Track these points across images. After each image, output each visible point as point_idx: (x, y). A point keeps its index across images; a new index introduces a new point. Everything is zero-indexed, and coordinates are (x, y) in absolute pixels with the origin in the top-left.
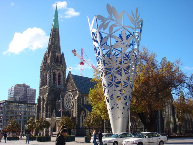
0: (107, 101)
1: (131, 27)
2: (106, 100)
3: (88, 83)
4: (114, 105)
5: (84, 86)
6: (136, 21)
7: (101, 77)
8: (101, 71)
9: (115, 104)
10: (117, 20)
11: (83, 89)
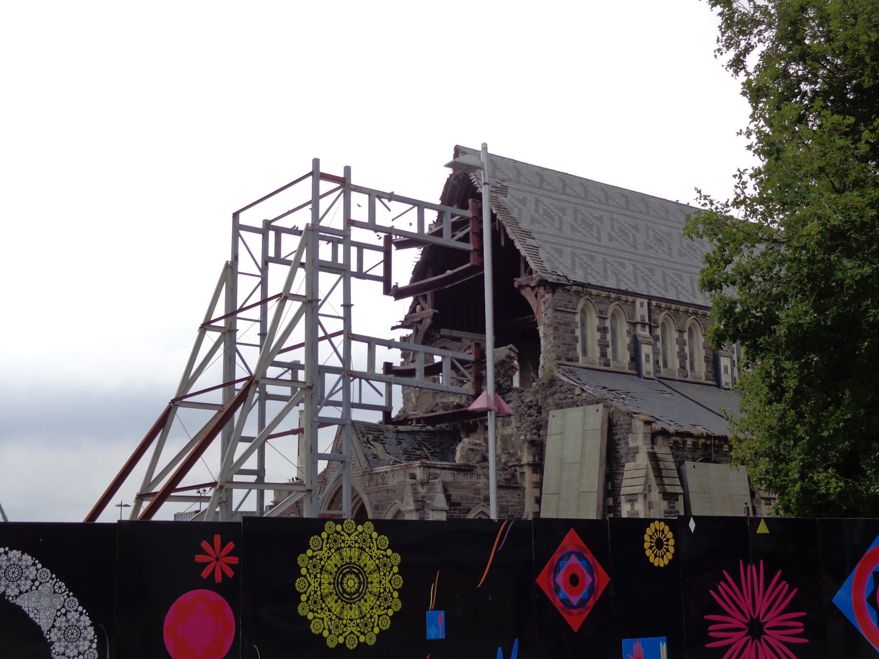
11: (560, 252)
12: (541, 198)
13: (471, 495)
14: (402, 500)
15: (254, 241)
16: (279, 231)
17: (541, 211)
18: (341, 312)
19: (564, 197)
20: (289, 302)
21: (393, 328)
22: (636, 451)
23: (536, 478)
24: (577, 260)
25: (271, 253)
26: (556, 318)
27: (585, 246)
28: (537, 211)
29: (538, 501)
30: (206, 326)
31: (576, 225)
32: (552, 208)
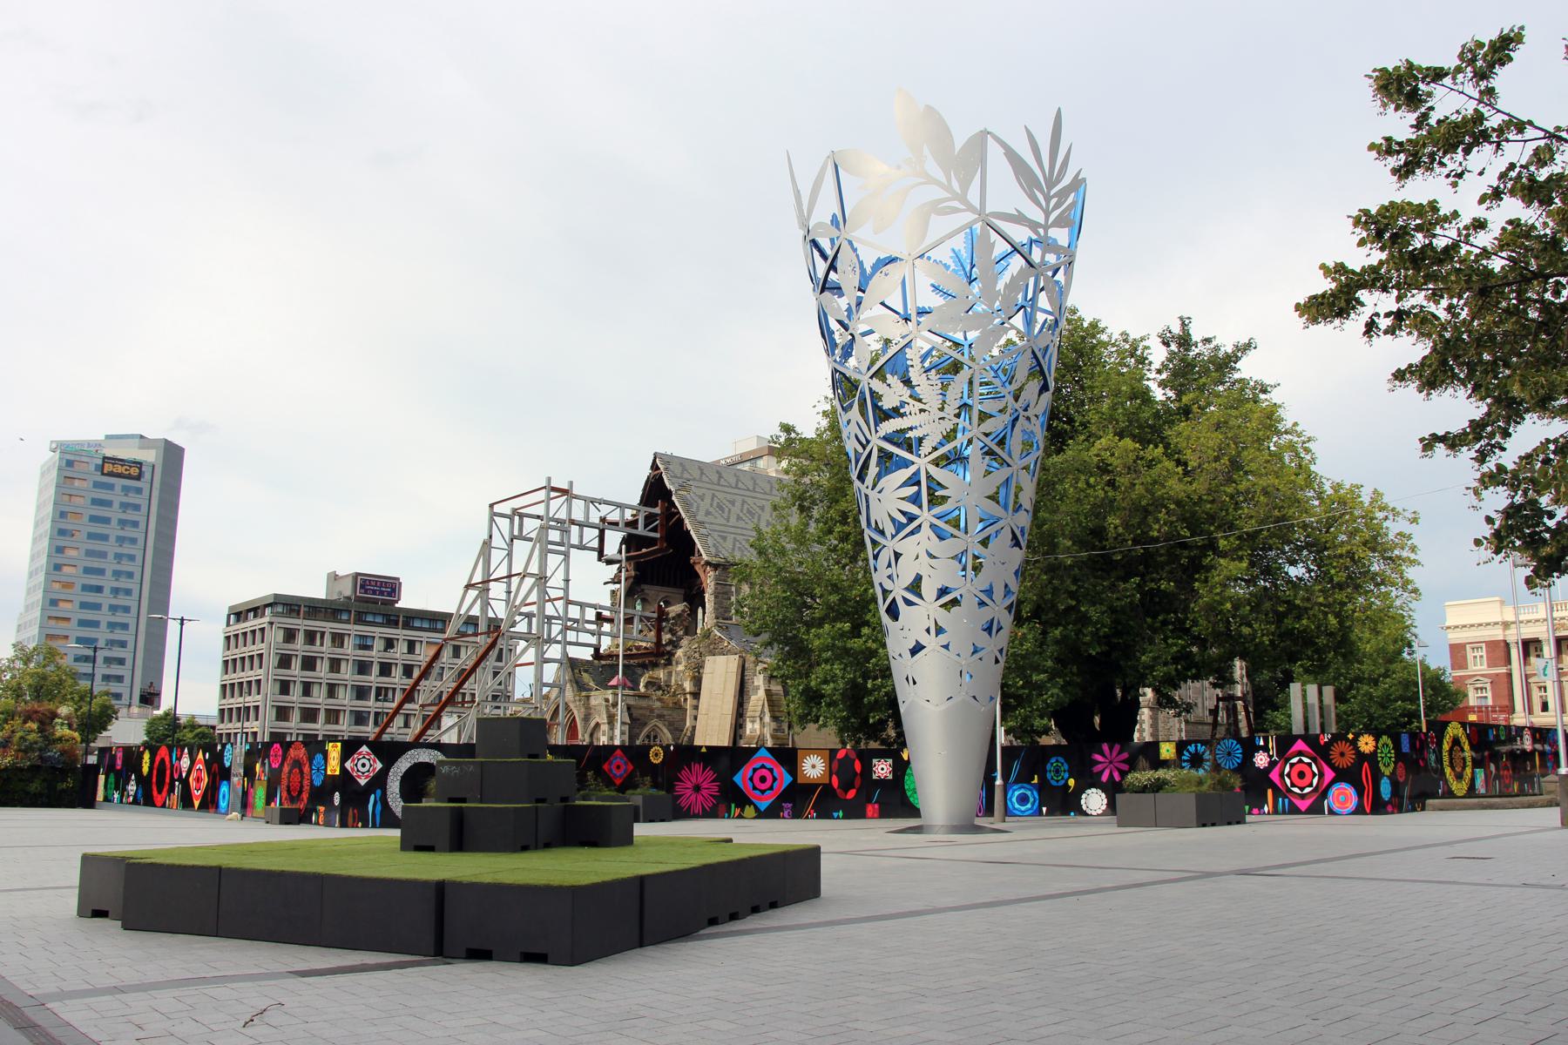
0: (887, 611)
1: (1019, 219)
2: (882, 608)
3: (749, 501)
4: (928, 631)
5: (733, 520)
6: (1051, 183)
7: (857, 483)
8: (860, 449)
9: (933, 631)
10: (949, 180)
11: (724, 538)
12: (717, 494)
13: (648, 713)
14: (599, 715)
15: (504, 523)
16: (521, 516)
17: (715, 504)
18: (562, 585)
19: (736, 491)
20: (526, 579)
21: (605, 583)
22: (758, 688)
23: (695, 702)
24: (738, 545)
25: (516, 533)
26: (716, 589)
27: (745, 532)
28: (711, 505)
29: (696, 718)
30: (469, 586)
31: (741, 515)
32: (725, 501)
